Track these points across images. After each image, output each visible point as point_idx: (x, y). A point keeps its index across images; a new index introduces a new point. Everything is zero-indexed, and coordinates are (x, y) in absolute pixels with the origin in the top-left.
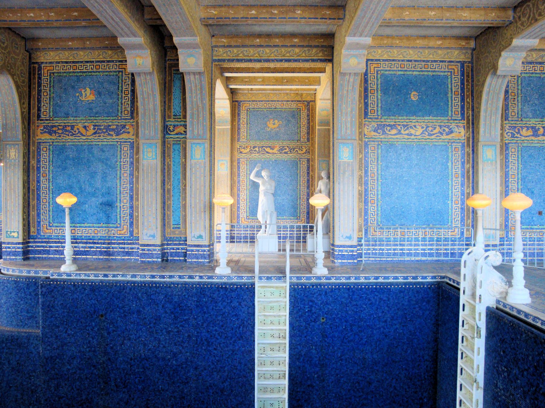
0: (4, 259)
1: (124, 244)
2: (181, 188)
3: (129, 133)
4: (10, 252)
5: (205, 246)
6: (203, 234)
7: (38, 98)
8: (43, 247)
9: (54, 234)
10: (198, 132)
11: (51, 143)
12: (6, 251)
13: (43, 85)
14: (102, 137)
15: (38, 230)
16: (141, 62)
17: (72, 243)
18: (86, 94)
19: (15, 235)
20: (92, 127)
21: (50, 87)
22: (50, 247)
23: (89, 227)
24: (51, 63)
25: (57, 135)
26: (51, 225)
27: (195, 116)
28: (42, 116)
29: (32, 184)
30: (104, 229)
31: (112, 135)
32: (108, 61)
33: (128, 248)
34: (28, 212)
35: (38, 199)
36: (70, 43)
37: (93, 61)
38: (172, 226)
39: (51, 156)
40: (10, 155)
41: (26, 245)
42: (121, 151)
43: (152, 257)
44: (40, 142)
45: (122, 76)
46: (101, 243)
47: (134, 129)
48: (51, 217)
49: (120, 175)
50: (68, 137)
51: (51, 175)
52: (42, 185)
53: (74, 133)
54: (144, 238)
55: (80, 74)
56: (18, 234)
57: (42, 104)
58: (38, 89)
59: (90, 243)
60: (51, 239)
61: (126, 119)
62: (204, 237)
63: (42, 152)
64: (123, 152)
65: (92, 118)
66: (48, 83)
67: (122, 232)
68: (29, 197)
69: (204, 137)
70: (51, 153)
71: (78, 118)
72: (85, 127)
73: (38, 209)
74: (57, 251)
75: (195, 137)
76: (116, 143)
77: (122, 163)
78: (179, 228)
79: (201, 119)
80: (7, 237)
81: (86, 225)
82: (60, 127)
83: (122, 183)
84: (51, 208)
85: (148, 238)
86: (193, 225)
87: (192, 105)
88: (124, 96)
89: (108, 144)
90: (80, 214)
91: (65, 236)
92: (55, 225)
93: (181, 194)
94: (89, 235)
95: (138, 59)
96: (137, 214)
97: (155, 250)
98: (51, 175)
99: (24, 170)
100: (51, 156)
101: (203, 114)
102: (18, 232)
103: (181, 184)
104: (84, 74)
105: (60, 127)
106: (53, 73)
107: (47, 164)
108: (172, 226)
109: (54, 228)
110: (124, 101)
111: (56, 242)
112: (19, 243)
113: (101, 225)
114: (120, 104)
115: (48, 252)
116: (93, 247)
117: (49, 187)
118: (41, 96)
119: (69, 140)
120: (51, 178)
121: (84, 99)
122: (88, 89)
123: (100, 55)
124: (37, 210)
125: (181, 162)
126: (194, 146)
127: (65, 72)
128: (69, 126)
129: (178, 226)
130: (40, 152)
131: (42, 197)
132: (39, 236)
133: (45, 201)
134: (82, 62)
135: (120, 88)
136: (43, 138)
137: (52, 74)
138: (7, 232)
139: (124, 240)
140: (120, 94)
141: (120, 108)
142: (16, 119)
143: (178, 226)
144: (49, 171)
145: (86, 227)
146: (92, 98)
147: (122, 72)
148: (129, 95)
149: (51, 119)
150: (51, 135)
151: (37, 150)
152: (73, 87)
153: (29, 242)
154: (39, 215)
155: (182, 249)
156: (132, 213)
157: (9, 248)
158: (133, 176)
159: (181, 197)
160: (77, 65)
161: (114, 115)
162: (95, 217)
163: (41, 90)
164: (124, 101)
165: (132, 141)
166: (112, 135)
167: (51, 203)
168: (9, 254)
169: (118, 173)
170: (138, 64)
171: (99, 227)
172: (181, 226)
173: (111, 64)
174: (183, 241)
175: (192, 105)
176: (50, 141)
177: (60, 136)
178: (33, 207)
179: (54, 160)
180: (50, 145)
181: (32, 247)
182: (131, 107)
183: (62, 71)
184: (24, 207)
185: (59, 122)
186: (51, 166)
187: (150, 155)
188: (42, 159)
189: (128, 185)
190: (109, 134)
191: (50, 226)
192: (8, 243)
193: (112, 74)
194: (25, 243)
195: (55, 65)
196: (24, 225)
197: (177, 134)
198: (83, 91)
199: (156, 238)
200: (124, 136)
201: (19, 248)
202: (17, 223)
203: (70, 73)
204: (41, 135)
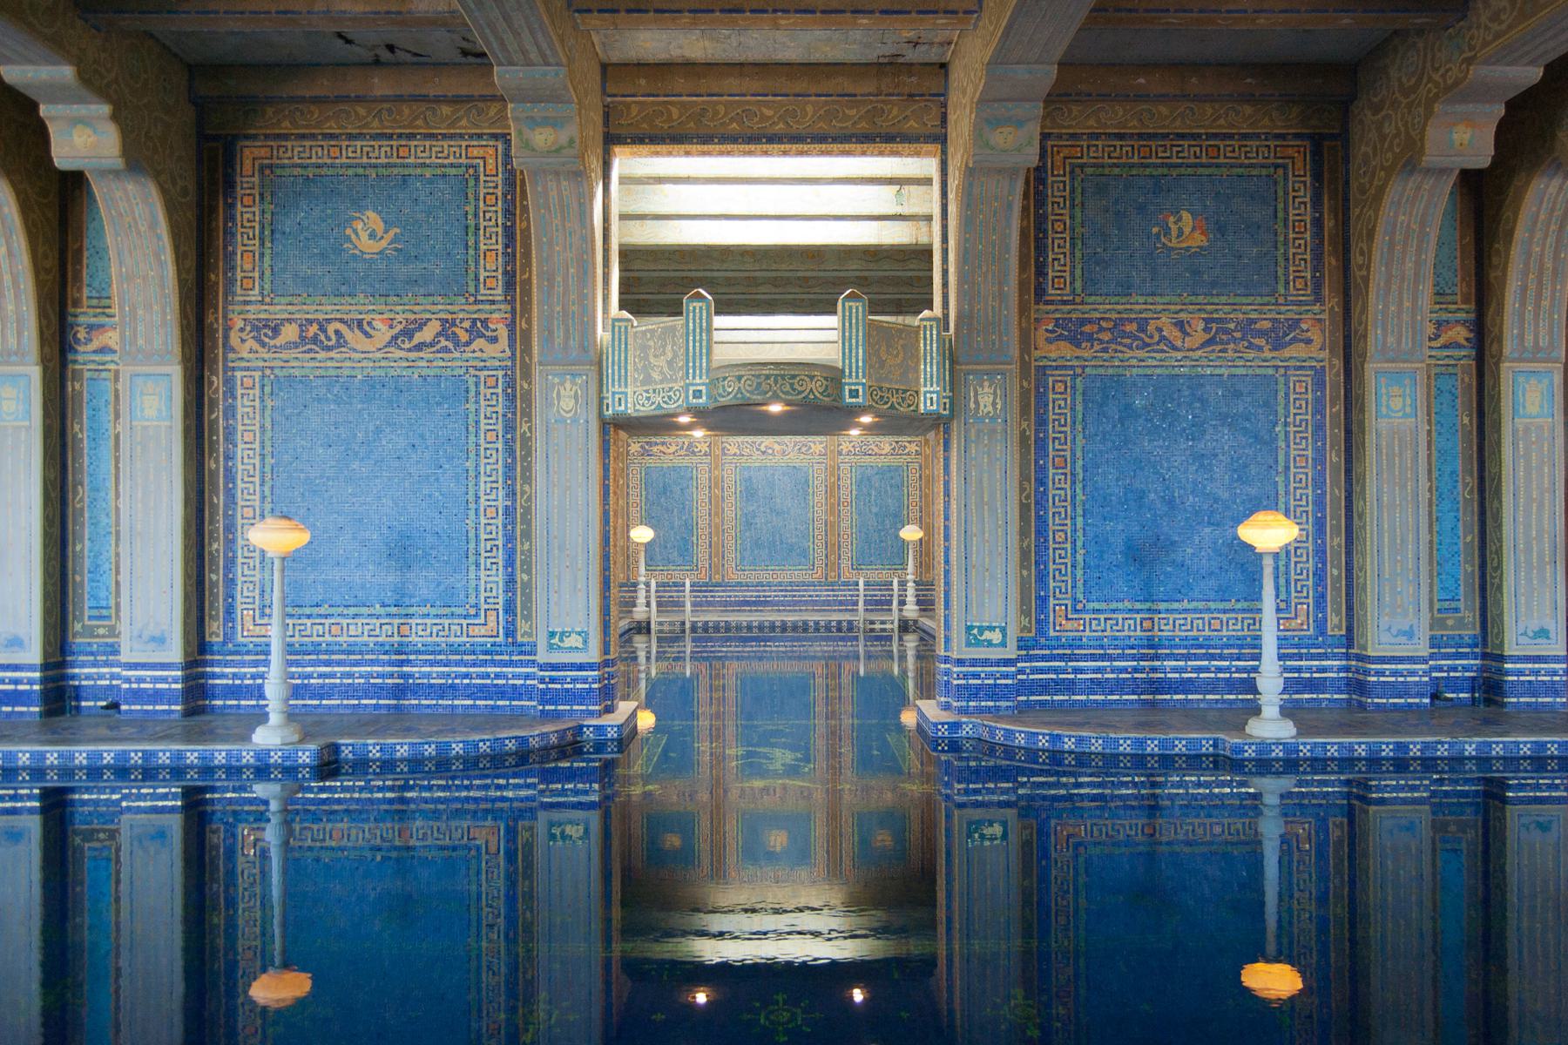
1: (1300, 657)
2: (1460, 498)
3: (1309, 342)
4: (979, 688)
5: (1556, 659)
6: (1550, 625)
7: (1037, 239)
8: (1056, 671)
9: (1087, 633)
10: (1536, 342)
11: (1079, 371)
13: (1050, 200)
14: (1230, 354)
15: (1038, 621)
16: (1467, 137)
17: (1281, 657)
18: (1180, 229)
19: (996, 637)
20: (1201, 325)
21: (1073, 206)
22: (1076, 671)
23: (1195, 610)
24: (1073, 136)
25: (1097, 347)
26: (1080, 606)
27: (1531, 293)
28: (1051, 291)
30: (1240, 616)
31: (1260, 349)
32: (1245, 136)
33: (1309, 669)
36: (1142, 81)
37: (1199, 136)
38: (1437, 606)
39: (1079, 408)
42: (1287, 395)
43: (1407, 694)
44: (1045, 367)
45: (1286, 179)
46: (1231, 658)
47: (1323, 331)
48: (1080, 584)
49: (1287, 461)
50: (1130, 354)
51: (1080, 463)
52: (1051, 493)
53: (1147, 340)
54: (1383, 640)
55: (1160, 171)
56: (1004, 636)
57: (1051, 256)
58: (1036, 213)
59: (1197, 657)
60: (1080, 647)
61: (1300, 303)
62: (1553, 635)
63: (1051, 396)
64: (1292, 397)
65: (1200, 299)
66: (1067, 193)
67: (1293, 624)
69: (1554, 354)
70: (1079, 398)
71: (1158, 299)
72: (1180, 325)
74: (1097, 682)
75: (1525, 355)
76: (1271, 372)
77: (1292, 429)
78: (1457, 610)
79: (1545, 303)
80: (968, 644)
81: (1185, 604)
82: (1104, 324)
83: (1292, 485)
84: (1080, 558)
85: (1393, 640)
86: (1523, 600)
87: (1527, 265)
88: (1291, 236)
89: (1250, 372)
90: (1168, 575)
91: (1259, 638)
92: (1091, 606)
93: (1461, 514)
94: (1195, 633)
95: (1461, 128)
96: (1335, 572)
97: (1413, 673)
98: (1080, 463)
100: (1079, 408)
101: (1554, 291)
102: (1003, 630)
103: (1460, 486)
104: (1175, 173)
105: (1104, 324)
106: (1082, 166)
107: (1068, 429)
108: (1437, 606)
109: (1087, 617)
110: (1292, 251)
111: (1093, 658)
112: (1007, 662)
113: (1232, 604)
114: (1281, 260)
115: (1070, 687)
116: (1207, 670)
117: (1074, 497)
118: (1045, 231)
119: (1134, 362)
120: (1079, 470)
121: (1174, 243)
122: (1186, 216)
123: (1219, 117)
125: (1459, 427)
126: (1521, 379)
127: (1116, 166)
128: (1131, 321)
129: (1454, 605)
130: (1045, 394)
132: (1043, 641)
133: (1060, 537)
134: (1165, 136)
135: (1281, 215)
136: (1053, 355)
137: (1078, 171)
139: (1297, 646)
140: (1280, 229)
141: (1280, 272)
142: (1001, 296)
143: (1454, 605)
144: (1073, 454)
145: (1186, 611)
146: (1199, 240)
147: (1285, 167)
148: (1308, 236)
149: (1078, 300)
150: (1078, 346)
151: (1037, 388)
152: (1141, 208)
155: (1465, 669)
156: (1324, 570)
157: (976, 676)
158: (1323, 463)
159: (1460, 524)
160: (1153, 144)
161: (1265, 290)
162: (1212, 583)
163: (1045, 217)
164: (1292, 251)
165: (1318, 365)
166: (1260, 349)
167: (1079, 544)
169: (1281, 458)
170: (1457, 143)
171: (1225, 611)
172: (1461, 605)
173: (1255, 143)
174: (1469, 646)
175: (1527, 265)
176: (1075, 363)
177: (1105, 350)
179: (1089, 420)
180: (1075, 376)
182: (1315, 269)
183: (1107, 160)
185: (1102, 308)
186: (1080, 437)
187: (1397, 403)
188: (1051, 417)
189: (1310, 491)
190: (1251, 346)
191: (1077, 611)
193: (1255, 172)
195: (1085, 144)
197: (1445, 347)
198: (1172, 219)
199: (1415, 640)
200: (1295, 351)
202: (1001, 601)
203: (1132, 166)
204: (1047, 347)
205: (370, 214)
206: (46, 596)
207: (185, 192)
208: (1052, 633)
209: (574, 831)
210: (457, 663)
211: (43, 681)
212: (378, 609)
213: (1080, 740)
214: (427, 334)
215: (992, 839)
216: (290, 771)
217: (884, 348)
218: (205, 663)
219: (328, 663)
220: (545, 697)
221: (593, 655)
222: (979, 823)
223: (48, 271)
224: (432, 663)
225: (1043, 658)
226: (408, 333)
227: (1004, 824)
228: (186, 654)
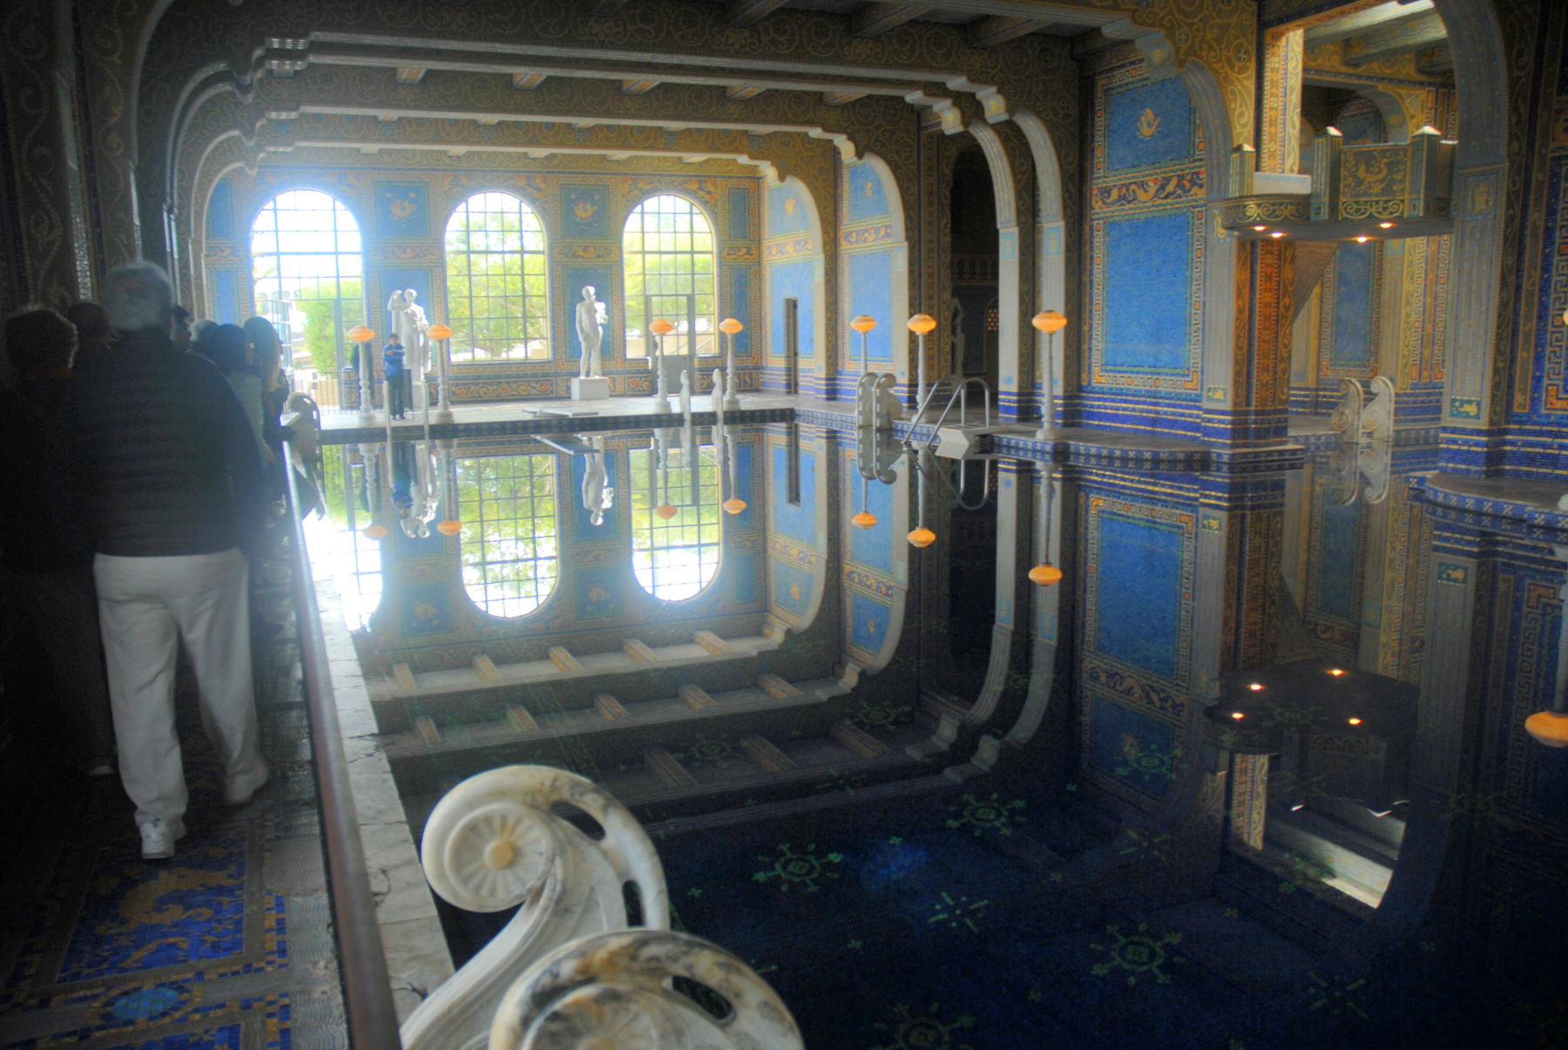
0: (1443, 470)
4: (1457, 452)
8: (1543, 445)
12: (1447, 450)
15: (1533, 400)
29: (1530, 277)
34: (1513, 351)
35: (1540, 318)
40: (1473, 202)
41: (1497, 439)
68: (1516, 313)
73: (1540, 345)
80: (1452, 415)
99: (1506, 239)
102: (1478, 404)
112: (1479, 432)
124: (1536, 346)
131: (1551, 312)
132: (1535, 418)
138: (1453, 401)
153: (1507, 432)
154: (1539, 360)
157: (1454, 442)
168: (1454, 456)
178: (1527, 337)
181: (1513, 444)
184: (1499, 339)
192: (1454, 430)
194: (1496, 432)
196: (1496, 386)
201: (1477, 444)
205: (1148, 111)
206: (1021, 355)
207: (1067, 116)
208: (1543, 411)
209: (1214, 524)
210: (1180, 406)
211: (1019, 401)
212: (1146, 369)
213: (1446, 495)
214: (1170, 188)
215: (1456, 580)
216: (1043, 452)
217: (1362, 168)
218: (1080, 398)
219: (1125, 401)
220: (1208, 432)
221: (1228, 406)
222: (1448, 567)
223: (1023, 173)
224: (1169, 405)
225: (1533, 433)
226: (1162, 187)
227: (1466, 569)
228: (1065, 390)
